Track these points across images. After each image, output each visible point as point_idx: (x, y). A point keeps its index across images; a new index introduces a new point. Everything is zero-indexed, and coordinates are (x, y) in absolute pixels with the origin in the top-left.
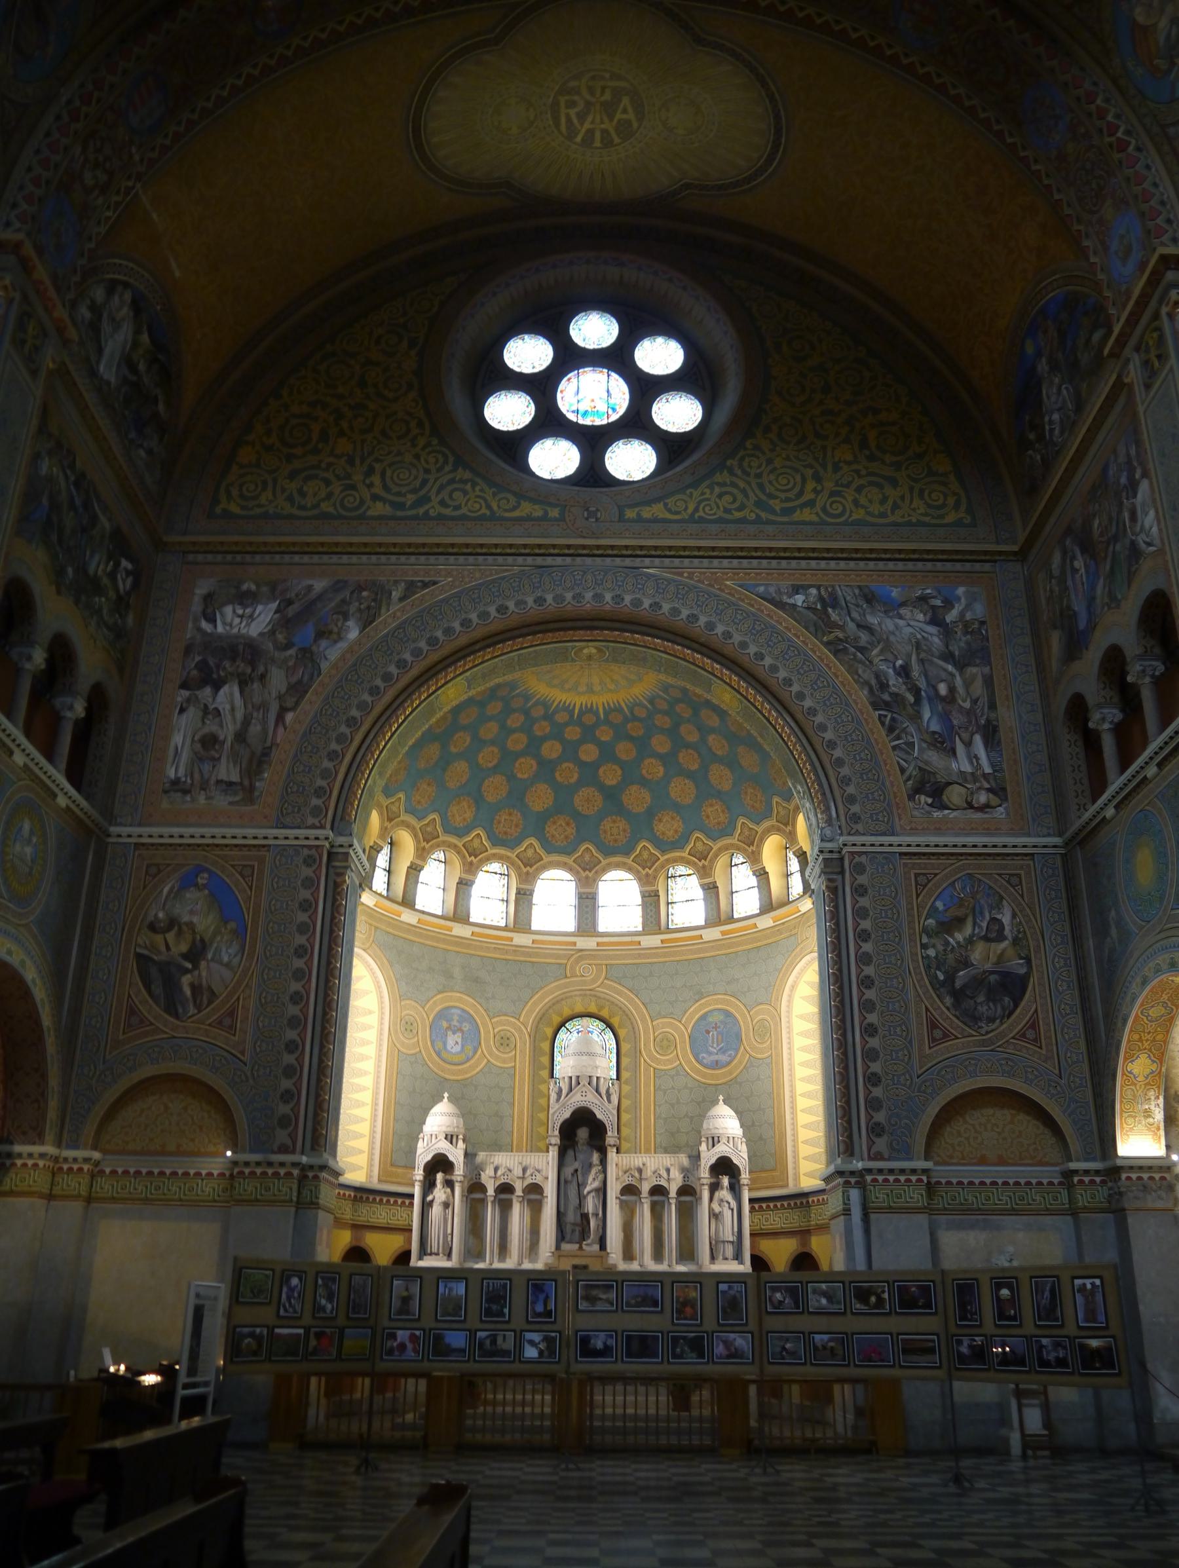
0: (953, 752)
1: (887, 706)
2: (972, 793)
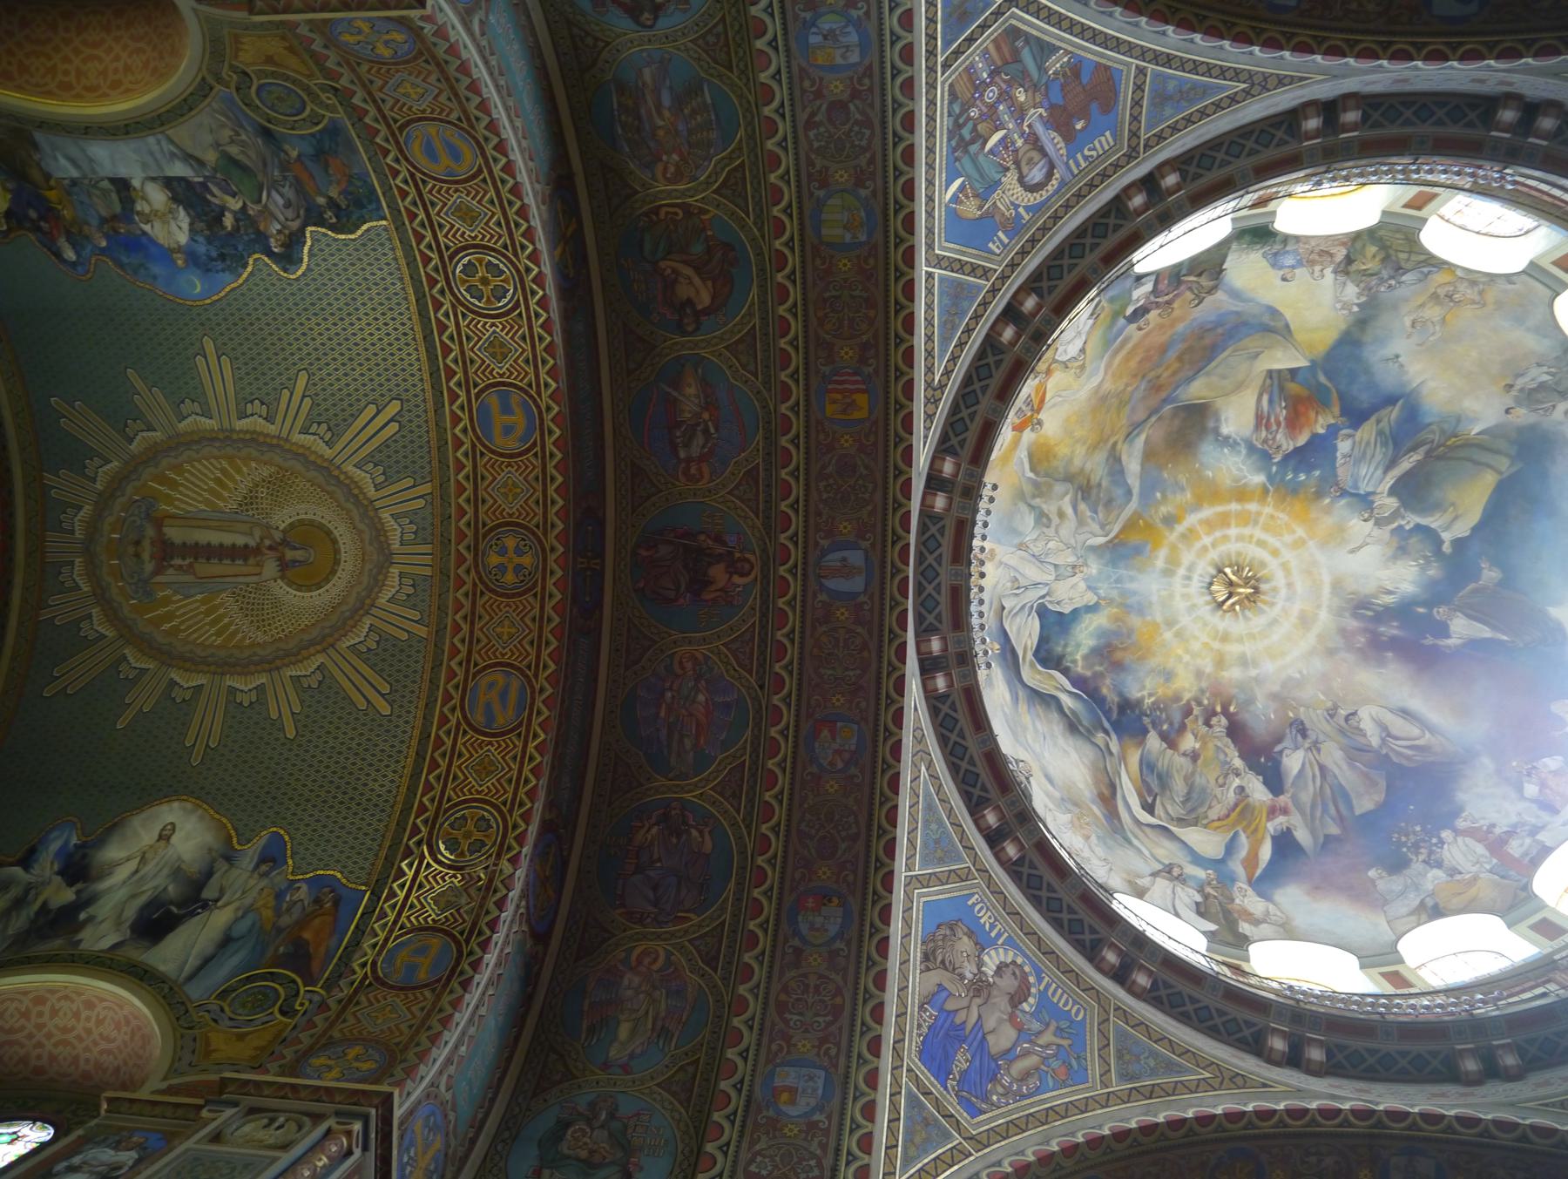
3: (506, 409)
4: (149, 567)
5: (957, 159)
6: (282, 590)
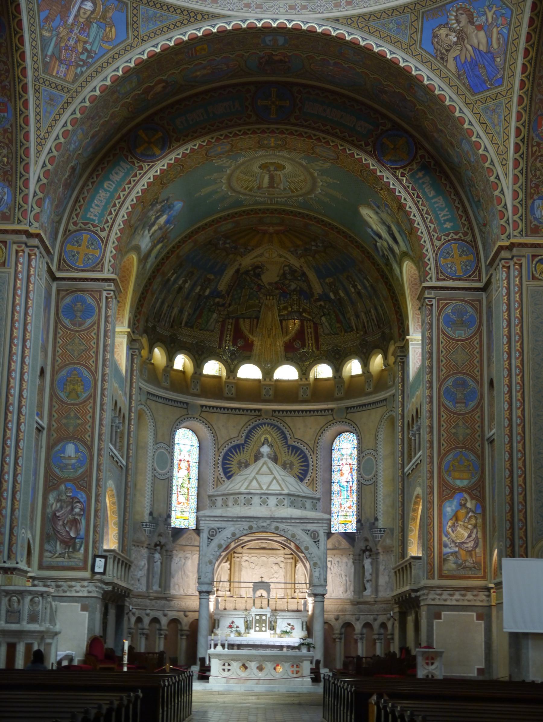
5: (95, 54)
6: (286, 171)
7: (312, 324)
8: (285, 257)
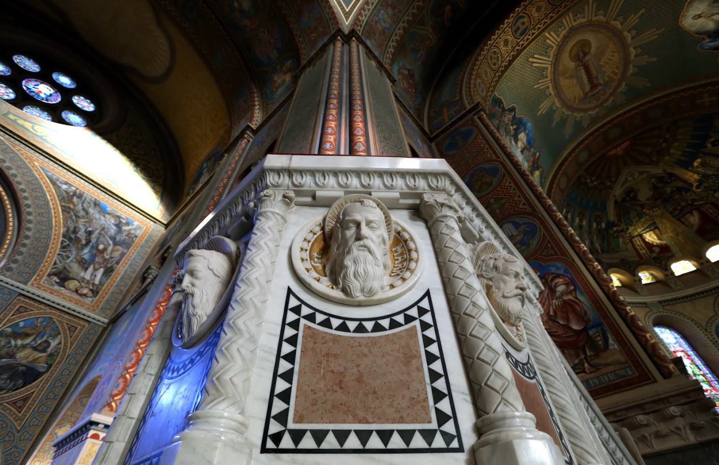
0: (86, 269)
1: (70, 239)
2: (82, 287)
3: (518, 28)
4: (600, 88)
6: (593, 50)
7: (709, 205)
8: (645, 172)
